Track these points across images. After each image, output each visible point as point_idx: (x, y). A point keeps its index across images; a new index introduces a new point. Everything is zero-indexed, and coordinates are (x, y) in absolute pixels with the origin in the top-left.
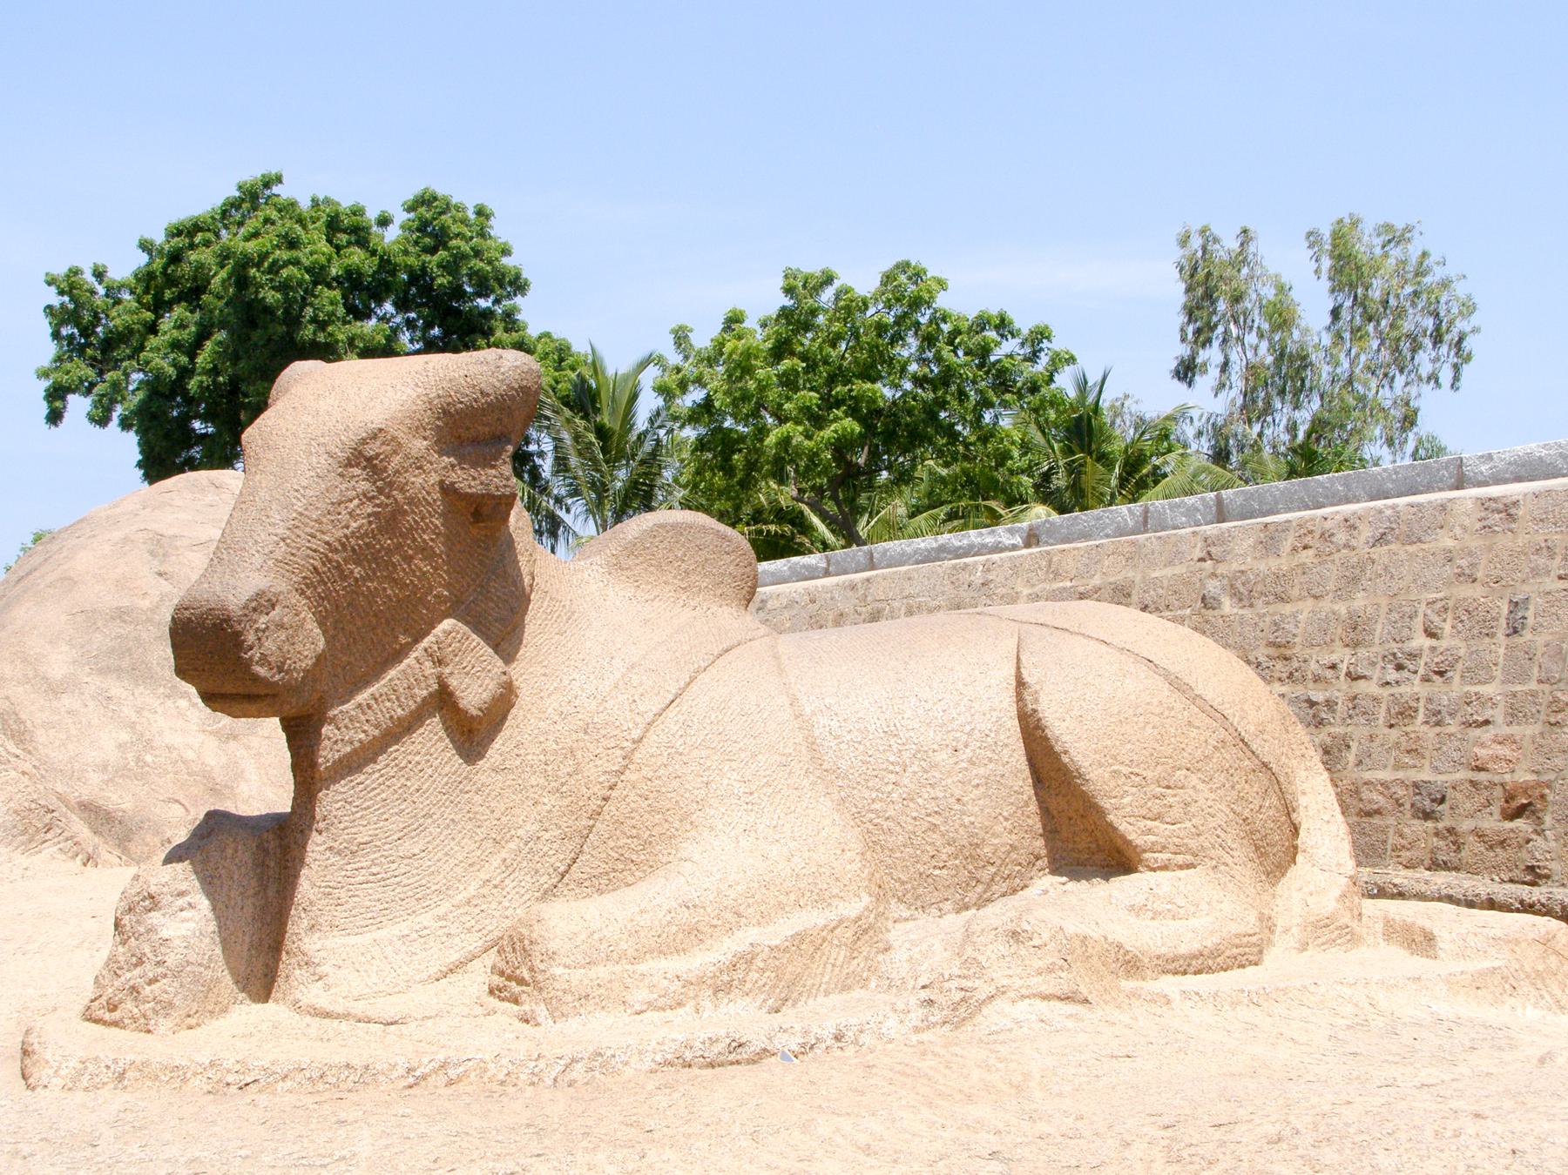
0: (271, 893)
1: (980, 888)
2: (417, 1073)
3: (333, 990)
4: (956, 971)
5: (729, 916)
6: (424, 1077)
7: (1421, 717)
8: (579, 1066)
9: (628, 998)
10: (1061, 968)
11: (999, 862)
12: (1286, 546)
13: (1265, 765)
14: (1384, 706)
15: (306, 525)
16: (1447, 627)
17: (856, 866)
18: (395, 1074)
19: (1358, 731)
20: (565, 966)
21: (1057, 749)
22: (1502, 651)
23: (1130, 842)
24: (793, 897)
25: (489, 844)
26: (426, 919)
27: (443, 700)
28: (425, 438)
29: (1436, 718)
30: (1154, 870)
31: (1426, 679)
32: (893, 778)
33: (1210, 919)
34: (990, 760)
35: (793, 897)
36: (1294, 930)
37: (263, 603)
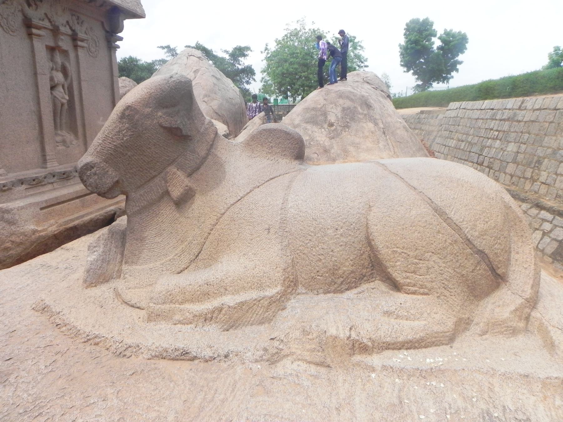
1: (336, 286)
2: (88, 338)
5: (222, 290)
6: (89, 340)
10: (318, 351)
11: (345, 277)
15: (108, 139)
17: (279, 274)
18: (84, 336)
20: (155, 304)
23: (398, 281)
24: (249, 285)
25: (180, 241)
26: (158, 263)
27: (167, 193)
28: (150, 108)
30: (408, 294)
32: (310, 238)
33: (424, 323)
34: (350, 235)
35: (249, 285)
36: (481, 324)
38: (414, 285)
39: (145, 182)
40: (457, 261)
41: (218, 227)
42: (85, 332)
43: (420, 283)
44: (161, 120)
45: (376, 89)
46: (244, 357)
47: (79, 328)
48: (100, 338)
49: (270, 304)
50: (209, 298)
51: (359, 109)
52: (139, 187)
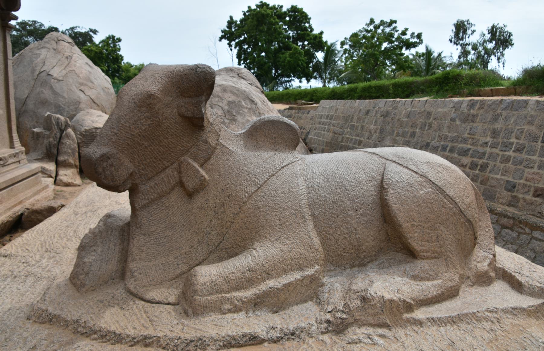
0: (125, 244)
2: (135, 340)
3: (137, 282)
4: (341, 308)
5: (264, 275)
7: (511, 162)
8: (192, 343)
9: (222, 308)
12: (476, 108)
13: (468, 220)
14: (500, 157)
16: (523, 137)
18: (128, 340)
19: (491, 163)
20: (201, 296)
21: (393, 215)
22: (539, 147)
23: (415, 249)
27: (181, 184)
28: (171, 97)
29: (515, 163)
31: (514, 151)
34: (369, 214)
35: (289, 267)
37: (104, 157)
38: (428, 252)
39: (157, 173)
40: (456, 229)
41: (242, 216)
42: (128, 336)
43: (432, 249)
44: (183, 110)
45: (251, 84)
46: (310, 332)
47: (117, 332)
48: (150, 338)
49: (311, 282)
50: (253, 284)
51: (243, 103)
52: (149, 179)
